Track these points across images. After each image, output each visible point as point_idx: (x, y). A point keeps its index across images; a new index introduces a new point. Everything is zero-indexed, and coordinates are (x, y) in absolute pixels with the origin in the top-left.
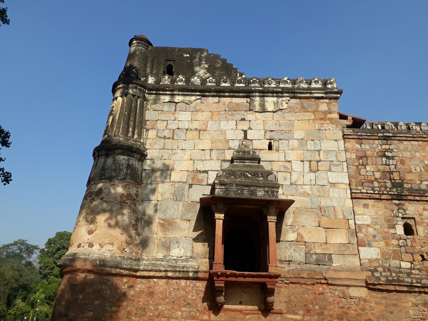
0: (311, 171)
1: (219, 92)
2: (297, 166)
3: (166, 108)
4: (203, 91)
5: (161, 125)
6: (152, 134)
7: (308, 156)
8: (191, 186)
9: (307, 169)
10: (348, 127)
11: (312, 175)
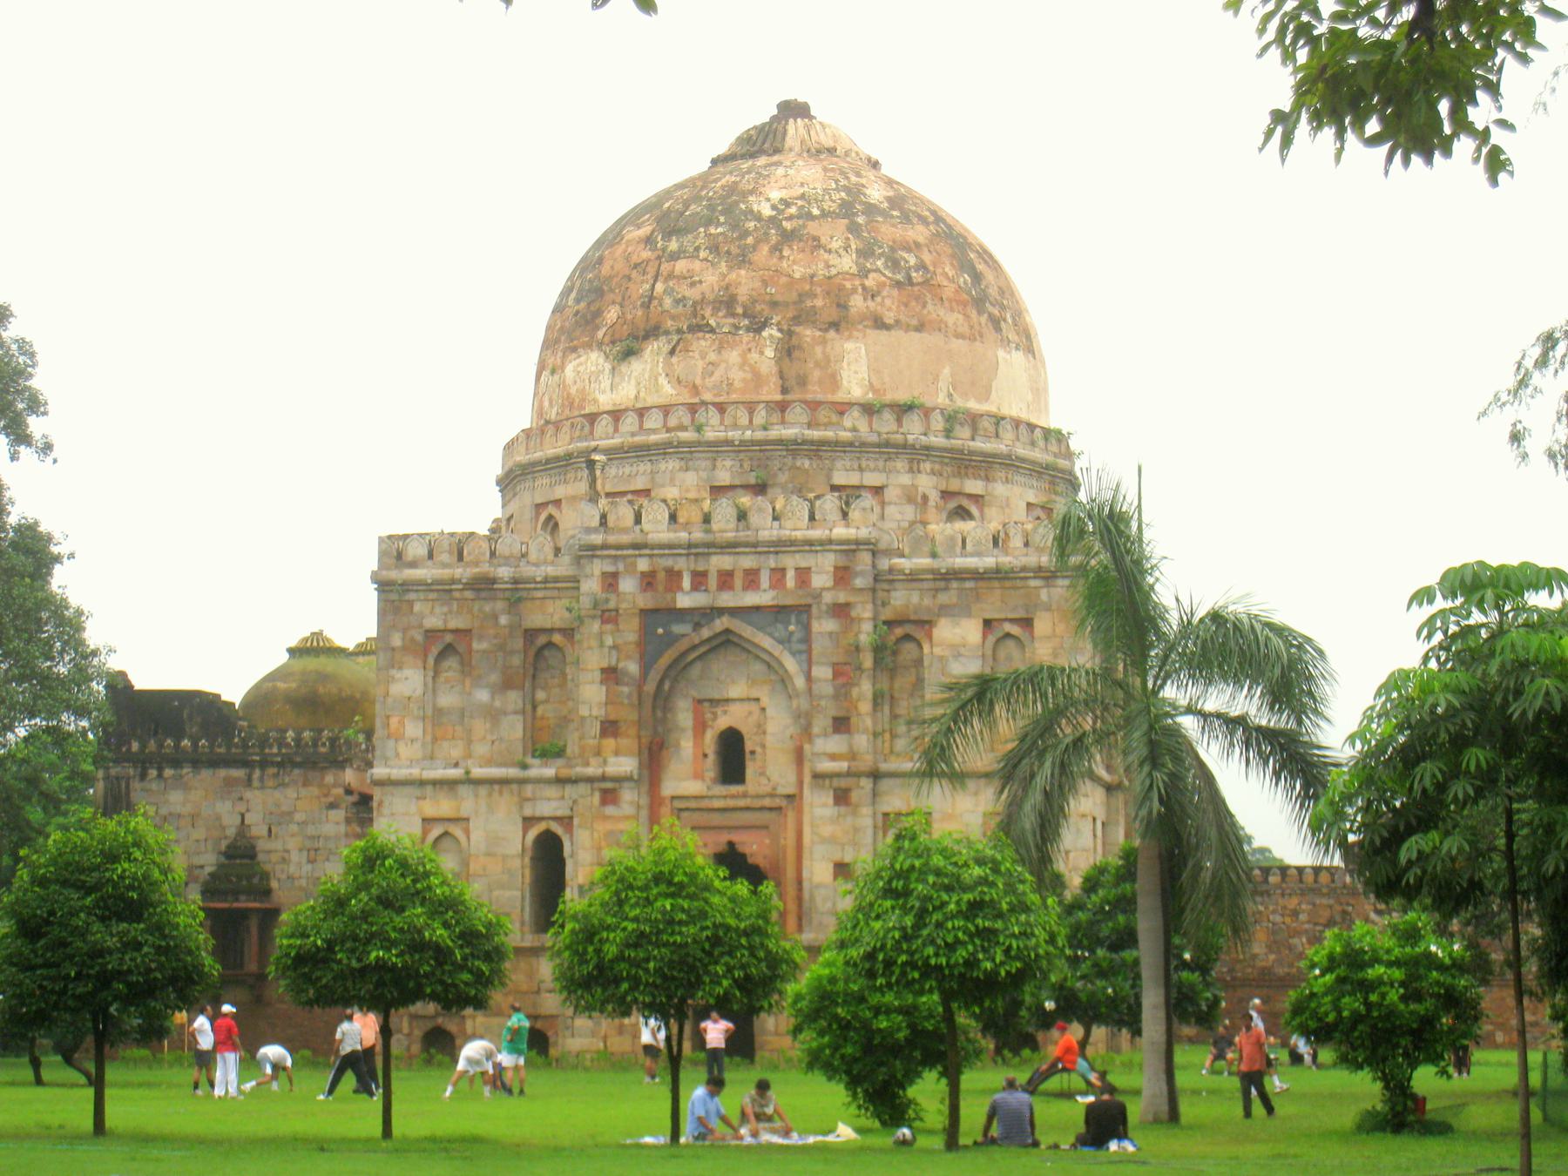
1: (215, 762)
2: (295, 857)
3: (154, 786)
4: (197, 763)
7: (308, 844)
8: (186, 884)
9: (304, 860)
11: (310, 867)
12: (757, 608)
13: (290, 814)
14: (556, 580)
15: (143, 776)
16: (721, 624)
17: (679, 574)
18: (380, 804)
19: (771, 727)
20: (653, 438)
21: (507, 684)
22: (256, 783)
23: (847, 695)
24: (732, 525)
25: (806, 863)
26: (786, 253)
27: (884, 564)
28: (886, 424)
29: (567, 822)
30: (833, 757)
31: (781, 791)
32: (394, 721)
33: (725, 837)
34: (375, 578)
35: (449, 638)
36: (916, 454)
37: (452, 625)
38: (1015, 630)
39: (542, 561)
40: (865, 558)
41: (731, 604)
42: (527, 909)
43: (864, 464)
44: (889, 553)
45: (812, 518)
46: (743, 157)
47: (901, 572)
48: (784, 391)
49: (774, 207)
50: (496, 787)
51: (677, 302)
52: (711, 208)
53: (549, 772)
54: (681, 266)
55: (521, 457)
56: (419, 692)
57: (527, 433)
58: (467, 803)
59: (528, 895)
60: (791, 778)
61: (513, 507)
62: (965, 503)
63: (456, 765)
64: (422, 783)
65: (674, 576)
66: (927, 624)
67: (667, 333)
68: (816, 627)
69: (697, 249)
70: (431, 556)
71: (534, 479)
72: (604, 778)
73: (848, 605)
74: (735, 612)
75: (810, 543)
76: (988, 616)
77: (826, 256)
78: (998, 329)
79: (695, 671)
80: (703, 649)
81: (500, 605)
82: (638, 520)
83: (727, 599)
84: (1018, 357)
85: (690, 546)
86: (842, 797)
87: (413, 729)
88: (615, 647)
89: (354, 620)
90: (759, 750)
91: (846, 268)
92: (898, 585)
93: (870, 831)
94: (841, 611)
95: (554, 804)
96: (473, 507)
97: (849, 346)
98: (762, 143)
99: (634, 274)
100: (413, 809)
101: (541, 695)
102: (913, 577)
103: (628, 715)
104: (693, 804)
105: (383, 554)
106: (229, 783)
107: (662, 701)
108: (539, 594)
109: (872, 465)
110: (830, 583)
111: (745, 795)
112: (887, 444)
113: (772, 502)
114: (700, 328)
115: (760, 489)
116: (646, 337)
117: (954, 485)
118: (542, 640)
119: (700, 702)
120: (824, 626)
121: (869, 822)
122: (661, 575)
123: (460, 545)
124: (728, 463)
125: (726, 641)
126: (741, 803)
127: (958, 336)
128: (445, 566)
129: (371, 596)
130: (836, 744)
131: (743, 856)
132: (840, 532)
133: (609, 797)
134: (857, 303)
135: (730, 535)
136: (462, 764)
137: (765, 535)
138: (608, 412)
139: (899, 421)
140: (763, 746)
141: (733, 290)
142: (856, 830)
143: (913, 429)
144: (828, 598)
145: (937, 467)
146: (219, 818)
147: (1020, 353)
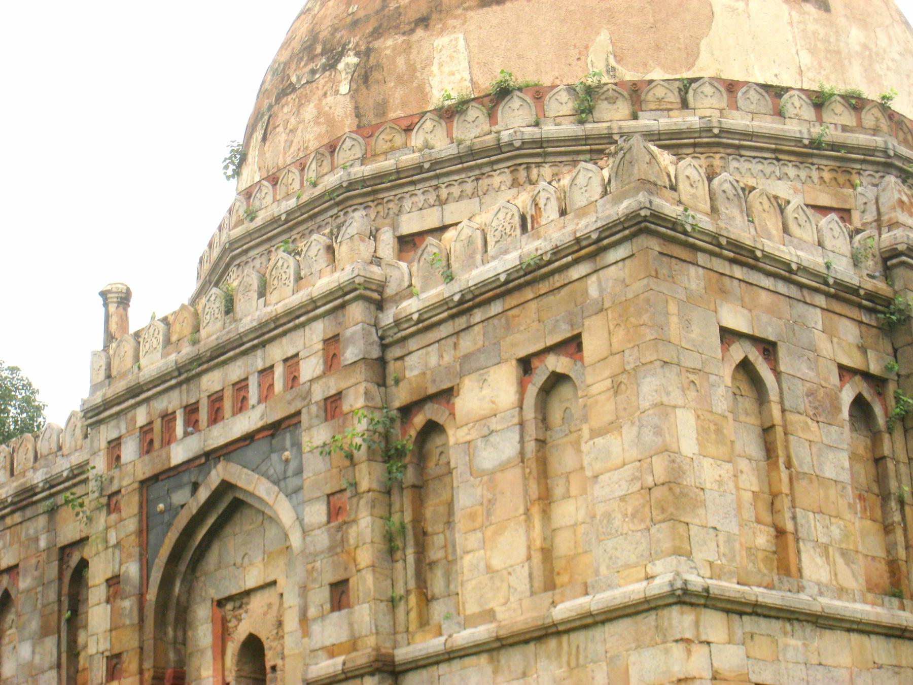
12: (249, 438)
30: (331, 651)
41: (221, 442)
43: (444, 196)
66: (447, 395)
76: (522, 353)
80: (210, 521)
83: (219, 436)
85: (180, 369)
90: (279, 662)
94: (332, 405)
102: (425, 324)
112: (472, 153)
130: (331, 630)
139: (492, 115)
143: (515, 121)
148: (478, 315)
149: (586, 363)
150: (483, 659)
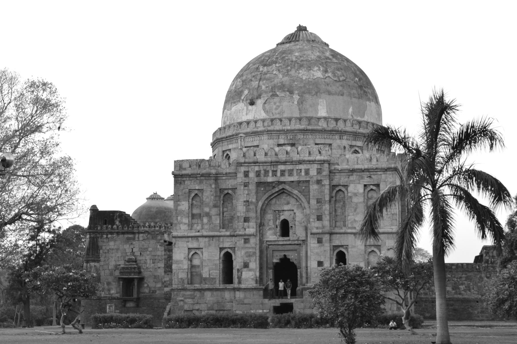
0: (153, 263)
1: (123, 233)
2: (148, 261)
4: (118, 233)
5: (104, 248)
6: (101, 251)
9: (151, 262)
10: (167, 245)
11: (153, 265)
13: (147, 248)
14: (230, 173)
15: (102, 237)
16: (281, 187)
17: (268, 171)
18: (175, 244)
19: (297, 219)
20: (259, 129)
21: (215, 206)
22: (137, 239)
23: (321, 208)
24: (285, 156)
25: (309, 262)
26: (300, 71)
27: (333, 168)
28: (332, 125)
29: (233, 249)
30: (317, 228)
31: (300, 239)
32: (179, 218)
33: (283, 254)
34: (173, 173)
35: (196, 192)
36: (341, 133)
37: (197, 188)
38: (374, 188)
39: (225, 168)
40: (326, 165)
42: (221, 276)
43: (325, 137)
44: (334, 164)
45: (310, 153)
46: (287, 43)
47: (338, 170)
48: (300, 113)
49: (296, 58)
50: (211, 238)
51: (267, 87)
52: (277, 58)
53: (228, 233)
54: (268, 75)
55: (219, 136)
56: (187, 208)
57: (220, 129)
58: (202, 242)
59: (221, 272)
60: (304, 235)
61: (216, 152)
62: (357, 149)
63: (199, 231)
64: (188, 237)
65: (266, 172)
66: (346, 186)
67: (263, 97)
68: (311, 187)
69: (273, 71)
70: (190, 166)
71: (222, 143)
72: (245, 235)
73: (321, 180)
74: (284, 183)
75: (309, 161)
76: (365, 184)
77: (313, 72)
78: (367, 95)
79: (273, 201)
81: (212, 181)
82: (255, 155)
83: (282, 179)
84: (373, 104)
85: (271, 162)
86: (320, 241)
87: (186, 220)
88: (248, 194)
89: (167, 189)
90: (293, 226)
91: (319, 76)
92: (337, 174)
93: (329, 251)
95: (230, 243)
96: (204, 152)
97: (320, 100)
98: (291, 39)
99: (253, 79)
100: (185, 246)
101: (225, 209)
102: (341, 171)
103: (252, 215)
104: (273, 243)
105: (175, 167)
106: (128, 239)
107: (263, 211)
108: (224, 178)
109: (328, 137)
110: (316, 174)
111: (289, 240)
113: (297, 148)
114: (274, 95)
115: (293, 145)
116: (257, 98)
117: (354, 143)
118: (226, 192)
119: (275, 211)
120: (314, 187)
121: (329, 248)
122: (262, 172)
123: (199, 163)
124: (283, 137)
125: (283, 192)
126: (288, 243)
127: (356, 97)
128: (194, 169)
129: (172, 179)
130: (318, 224)
131: (289, 259)
132: (319, 158)
133: (246, 241)
134: (323, 87)
135: (284, 159)
136: (200, 231)
137: (295, 159)
138: (245, 122)
140: (295, 225)
141: (284, 83)
142: (325, 251)
143: (341, 126)
144: (315, 179)
145: (348, 137)
146: (125, 250)
147: (373, 103)
148: (355, 173)
149: (381, 189)
150: (352, 235)
